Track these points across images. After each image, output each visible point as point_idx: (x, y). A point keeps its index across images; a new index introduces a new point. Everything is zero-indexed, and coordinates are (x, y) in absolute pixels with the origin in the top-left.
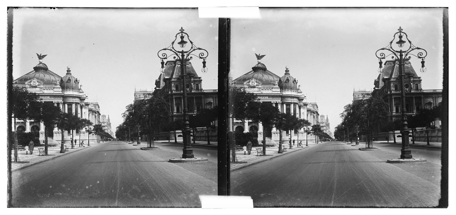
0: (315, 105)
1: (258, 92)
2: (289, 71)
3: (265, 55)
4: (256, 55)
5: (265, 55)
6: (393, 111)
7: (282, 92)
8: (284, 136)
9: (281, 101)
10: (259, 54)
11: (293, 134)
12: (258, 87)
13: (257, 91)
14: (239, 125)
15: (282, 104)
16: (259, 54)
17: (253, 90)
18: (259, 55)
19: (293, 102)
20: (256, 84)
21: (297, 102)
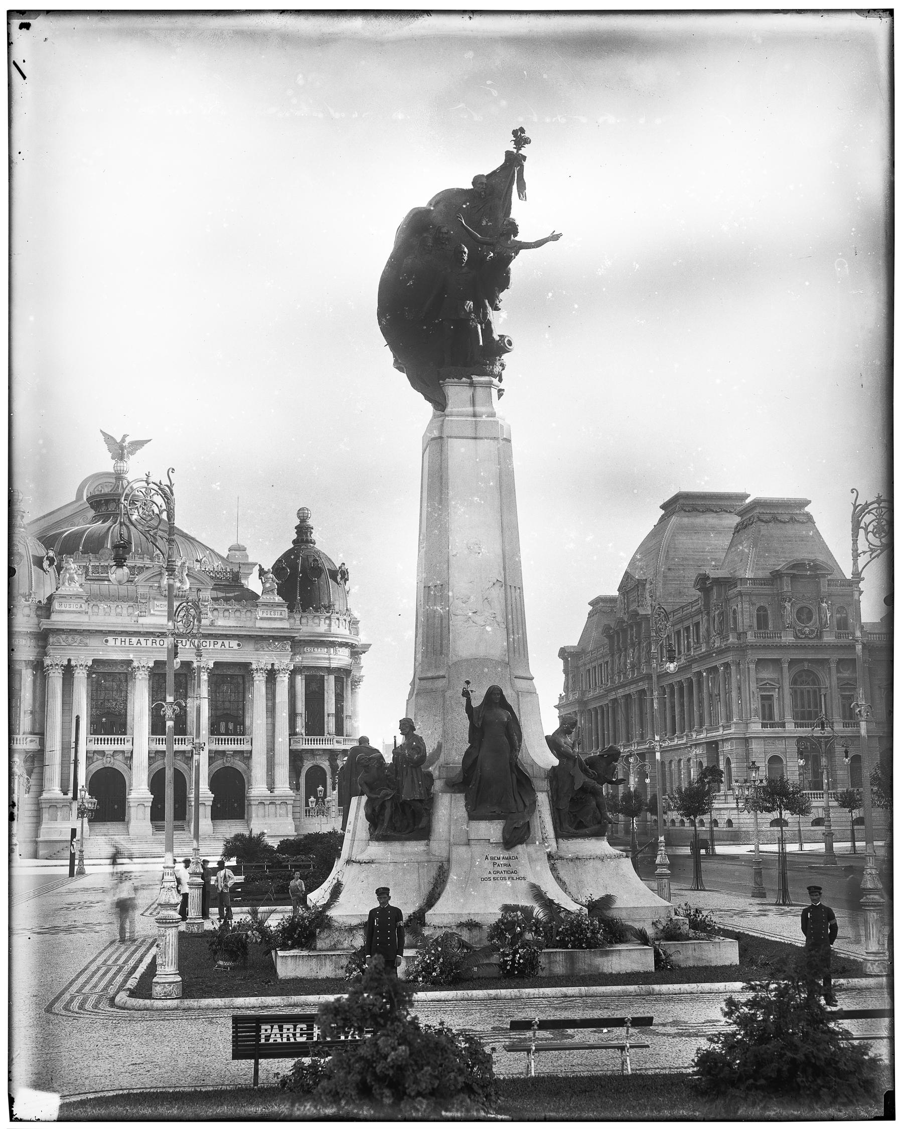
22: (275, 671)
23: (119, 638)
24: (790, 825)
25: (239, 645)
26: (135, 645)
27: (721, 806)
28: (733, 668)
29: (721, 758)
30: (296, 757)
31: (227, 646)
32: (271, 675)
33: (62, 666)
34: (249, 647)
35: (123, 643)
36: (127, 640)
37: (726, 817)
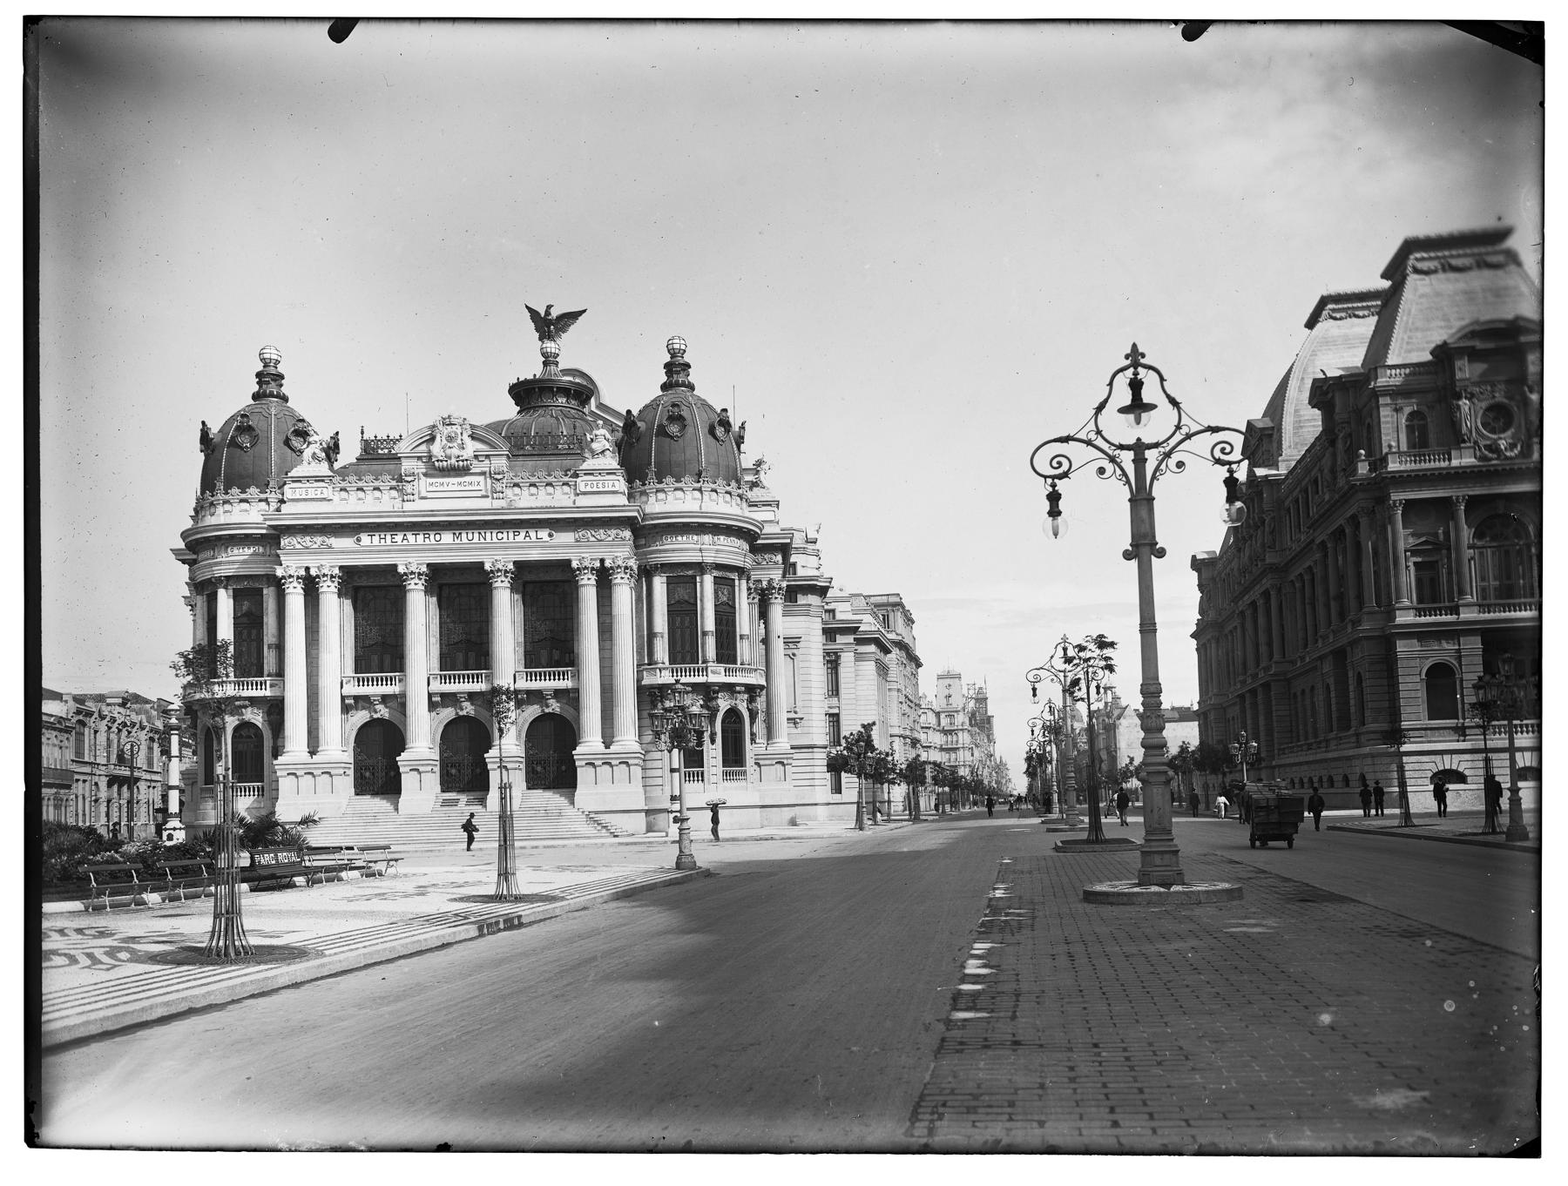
0: (890, 608)
1: (486, 504)
3: (585, 311)
4: (534, 314)
5: (585, 311)
6: (1398, 597)
7: (644, 498)
8: (659, 781)
10: (549, 307)
11: (714, 770)
12: (484, 466)
13: (479, 494)
14: (376, 712)
16: (549, 307)
17: (455, 488)
18: (548, 313)
19: (709, 560)
20: (472, 447)
21: (741, 564)
22: (608, 570)
23: (377, 534)
24: (1469, 779)
26: (399, 543)
27: (1351, 752)
28: (1364, 521)
29: (1350, 674)
30: (649, 696)
31: (534, 539)
32: (604, 577)
33: (298, 578)
34: (567, 537)
35: (383, 541)
36: (388, 537)
37: (1358, 770)
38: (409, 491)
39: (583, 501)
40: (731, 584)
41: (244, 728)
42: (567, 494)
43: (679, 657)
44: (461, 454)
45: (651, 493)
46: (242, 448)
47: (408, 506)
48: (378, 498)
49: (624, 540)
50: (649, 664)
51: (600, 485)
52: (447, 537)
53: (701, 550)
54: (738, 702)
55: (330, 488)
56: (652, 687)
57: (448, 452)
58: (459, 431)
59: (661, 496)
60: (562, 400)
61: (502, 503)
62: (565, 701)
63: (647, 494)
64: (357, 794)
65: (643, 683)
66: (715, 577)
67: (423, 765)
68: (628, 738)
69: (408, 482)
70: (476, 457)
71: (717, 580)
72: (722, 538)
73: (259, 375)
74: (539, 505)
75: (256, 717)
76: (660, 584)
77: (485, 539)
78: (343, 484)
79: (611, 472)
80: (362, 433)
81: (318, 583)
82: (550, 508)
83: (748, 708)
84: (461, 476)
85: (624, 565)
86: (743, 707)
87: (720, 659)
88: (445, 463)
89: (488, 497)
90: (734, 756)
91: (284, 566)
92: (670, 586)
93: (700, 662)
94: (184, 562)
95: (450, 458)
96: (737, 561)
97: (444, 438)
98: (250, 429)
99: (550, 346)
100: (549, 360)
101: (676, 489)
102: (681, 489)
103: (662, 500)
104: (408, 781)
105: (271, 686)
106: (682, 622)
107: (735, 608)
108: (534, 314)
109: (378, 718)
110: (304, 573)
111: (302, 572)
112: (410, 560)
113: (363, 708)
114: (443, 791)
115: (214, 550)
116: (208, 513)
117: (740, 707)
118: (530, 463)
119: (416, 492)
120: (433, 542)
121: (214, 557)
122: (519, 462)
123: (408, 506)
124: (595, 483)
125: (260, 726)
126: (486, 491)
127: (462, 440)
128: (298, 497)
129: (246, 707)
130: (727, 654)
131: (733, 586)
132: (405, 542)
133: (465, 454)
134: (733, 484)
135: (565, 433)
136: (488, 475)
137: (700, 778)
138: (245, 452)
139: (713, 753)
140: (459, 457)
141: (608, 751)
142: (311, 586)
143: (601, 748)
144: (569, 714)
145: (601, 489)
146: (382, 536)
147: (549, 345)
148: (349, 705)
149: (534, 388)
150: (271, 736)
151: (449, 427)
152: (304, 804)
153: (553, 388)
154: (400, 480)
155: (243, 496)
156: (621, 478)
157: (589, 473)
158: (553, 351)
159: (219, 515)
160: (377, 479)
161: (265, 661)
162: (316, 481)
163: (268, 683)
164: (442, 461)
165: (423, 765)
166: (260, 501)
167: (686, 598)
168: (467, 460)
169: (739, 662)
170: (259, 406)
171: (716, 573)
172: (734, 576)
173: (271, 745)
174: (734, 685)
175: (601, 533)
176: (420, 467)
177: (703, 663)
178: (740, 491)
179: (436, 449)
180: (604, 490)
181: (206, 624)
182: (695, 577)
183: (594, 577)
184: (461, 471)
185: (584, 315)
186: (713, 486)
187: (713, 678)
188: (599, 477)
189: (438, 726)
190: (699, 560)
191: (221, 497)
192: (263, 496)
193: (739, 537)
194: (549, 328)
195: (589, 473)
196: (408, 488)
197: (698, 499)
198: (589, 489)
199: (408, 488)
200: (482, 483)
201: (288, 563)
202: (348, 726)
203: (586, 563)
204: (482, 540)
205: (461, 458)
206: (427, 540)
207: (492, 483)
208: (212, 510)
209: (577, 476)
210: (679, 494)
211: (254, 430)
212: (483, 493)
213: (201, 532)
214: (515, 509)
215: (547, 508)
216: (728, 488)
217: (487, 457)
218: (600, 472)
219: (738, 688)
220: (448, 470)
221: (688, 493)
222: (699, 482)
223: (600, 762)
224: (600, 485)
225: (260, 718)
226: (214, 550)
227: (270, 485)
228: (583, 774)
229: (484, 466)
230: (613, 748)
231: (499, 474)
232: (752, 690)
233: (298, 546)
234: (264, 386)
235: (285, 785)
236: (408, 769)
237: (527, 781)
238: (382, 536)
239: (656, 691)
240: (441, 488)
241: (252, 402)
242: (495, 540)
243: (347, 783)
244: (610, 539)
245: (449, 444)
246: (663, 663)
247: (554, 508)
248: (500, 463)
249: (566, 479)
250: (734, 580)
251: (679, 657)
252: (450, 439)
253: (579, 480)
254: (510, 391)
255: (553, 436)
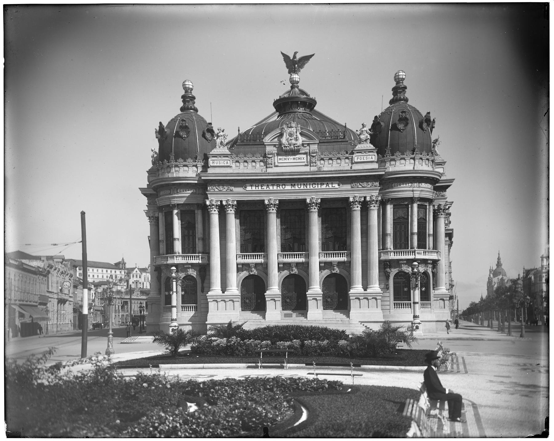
1: (307, 169)
2: (405, 88)
3: (313, 55)
4: (286, 57)
5: (313, 55)
9: (379, 194)
10: (296, 53)
12: (306, 149)
13: (304, 164)
15: (383, 204)
16: (296, 53)
17: (292, 161)
18: (295, 57)
20: (301, 139)
21: (430, 197)
22: (367, 202)
23: (254, 184)
25: (339, 185)
26: (265, 189)
30: (385, 265)
32: (365, 206)
34: (348, 187)
35: (257, 188)
38: (270, 162)
39: (355, 167)
40: (425, 207)
41: (188, 278)
42: (347, 163)
43: (398, 246)
44: (296, 142)
45: (388, 161)
46: (182, 138)
47: (269, 170)
48: (254, 166)
49: (376, 187)
50: (383, 249)
51: (365, 158)
52: (288, 187)
53: (413, 191)
54: (428, 268)
55: (231, 161)
56: (385, 261)
57: (290, 142)
58: (295, 131)
59: (393, 163)
60: (301, 110)
61: (314, 169)
62: (342, 267)
63: (385, 162)
64: (242, 310)
65: (381, 259)
66: (418, 204)
67: (277, 297)
68: (375, 287)
69: (269, 158)
70: (303, 145)
71: (419, 207)
72: (423, 184)
73: (183, 97)
74: (333, 169)
75: (193, 273)
76: (390, 209)
77: (307, 187)
78: (237, 159)
79: (370, 151)
80: (239, 131)
81: (225, 209)
82: (341, 171)
83: (432, 271)
84: (295, 155)
85: (376, 199)
86: (430, 271)
87: (419, 247)
88: (288, 148)
89: (308, 165)
90: (425, 296)
91: (210, 200)
92: (395, 209)
93: (409, 248)
94: (145, 195)
95: (291, 145)
96: (429, 195)
97: (287, 135)
98: (186, 128)
99: (296, 77)
100: (294, 84)
101: (401, 159)
102: (404, 159)
103: (393, 165)
104: (270, 305)
105: (202, 258)
106: (400, 228)
107: (426, 220)
108: (286, 57)
109: (253, 275)
110: (219, 203)
111: (219, 203)
112: (271, 198)
113: (246, 270)
114: (283, 310)
115: (170, 190)
116: (166, 171)
117: (428, 271)
118: (324, 147)
119: (273, 163)
120: (281, 189)
121: (170, 194)
122: (324, 147)
123: (269, 170)
124: (362, 157)
125: (195, 276)
126: (307, 162)
127: (296, 135)
128: (215, 165)
129: (189, 268)
130: (422, 245)
131: (426, 209)
132: (268, 189)
133: (298, 143)
134: (430, 154)
135: (340, 130)
136: (308, 154)
137: (409, 306)
138: (184, 140)
139: (416, 295)
140: (295, 144)
141: (366, 292)
142: (222, 210)
143: (362, 290)
144: (344, 273)
145: (365, 160)
146: (257, 185)
147: (294, 76)
148: (241, 268)
149: (289, 102)
150: (201, 282)
151: (290, 129)
152: (221, 315)
153: (298, 101)
154: (265, 156)
155: (185, 163)
156: (376, 154)
157: (360, 151)
158: (297, 80)
159: (173, 173)
160: (253, 156)
161: (197, 246)
162: (224, 157)
163: (200, 256)
164: (286, 147)
165: (277, 297)
166: (193, 166)
167: (403, 216)
168: (299, 146)
169: (427, 248)
170: (187, 115)
171: (418, 203)
172: (427, 204)
173: (201, 286)
174: (427, 260)
175: (365, 184)
176: (274, 150)
177: (411, 249)
178: (433, 158)
179: (284, 140)
180: (368, 160)
181: (164, 227)
182: (407, 205)
183: (360, 206)
184: (295, 152)
185: (313, 57)
186: (420, 156)
187: (418, 257)
188: (364, 154)
189: (281, 279)
190: (411, 196)
191: (173, 163)
192: (195, 164)
193: (426, 183)
194: (295, 66)
195: (360, 151)
196: (269, 161)
197: (412, 163)
198: (359, 160)
199: (269, 161)
200: (305, 158)
201: (212, 198)
202: (239, 277)
203: (357, 199)
204: (305, 188)
205: (296, 145)
206: (278, 187)
207: (310, 158)
208: (169, 170)
209: (353, 154)
210: (403, 161)
211: (188, 128)
212: (306, 163)
213: (167, 181)
214: (324, 171)
215: (339, 171)
216: (428, 157)
217: (308, 144)
218: (365, 151)
219: (429, 262)
220: (289, 152)
221: (407, 160)
222: (413, 154)
223: (362, 298)
224: (365, 158)
225: (195, 273)
226: (170, 190)
227: (198, 158)
228: (354, 304)
229: (306, 149)
230: (369, 291)
231: (314, 153)
232: (435, 263)
233: (216, 190)
234: (187, 103)
235: (212, 306)
236: (270, 299)
237: (323, 306)
238: (257, 185)
239: (388, 263)
240: (285, 161)
241: (180, 112)
242: (311, 187)
243: (238, 305)
244: (369, 186)
245: (290, 138)
246: (390, 249)
247: (343, 171)
248: (314, 147)
249: (347, 155)
250: (426, 206)
251: (398, 246)
252: (291, 135)
253: (354, 156)
254: (274, 104)
255: (334, 132)
